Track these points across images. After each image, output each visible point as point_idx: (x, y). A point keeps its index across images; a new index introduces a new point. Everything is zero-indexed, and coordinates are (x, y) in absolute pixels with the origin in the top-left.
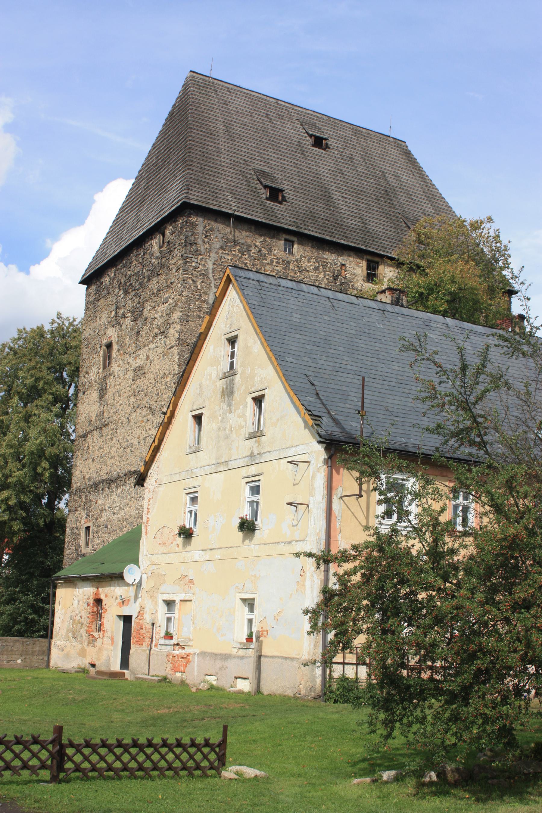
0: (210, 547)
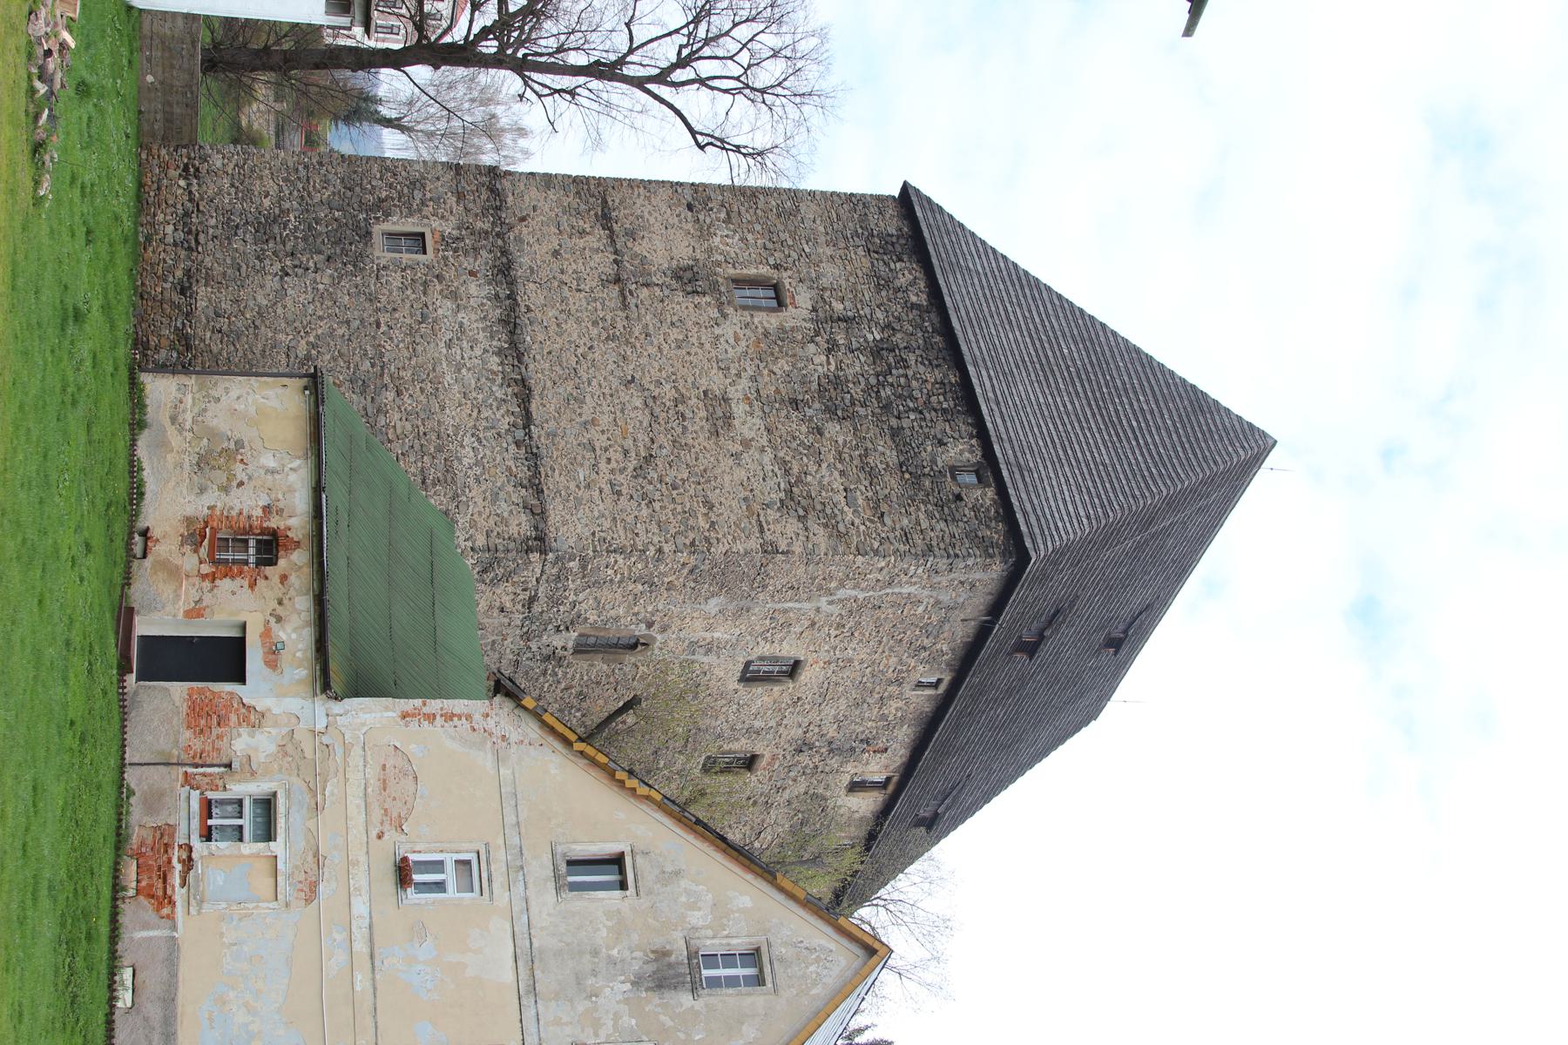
0: (377, 952)
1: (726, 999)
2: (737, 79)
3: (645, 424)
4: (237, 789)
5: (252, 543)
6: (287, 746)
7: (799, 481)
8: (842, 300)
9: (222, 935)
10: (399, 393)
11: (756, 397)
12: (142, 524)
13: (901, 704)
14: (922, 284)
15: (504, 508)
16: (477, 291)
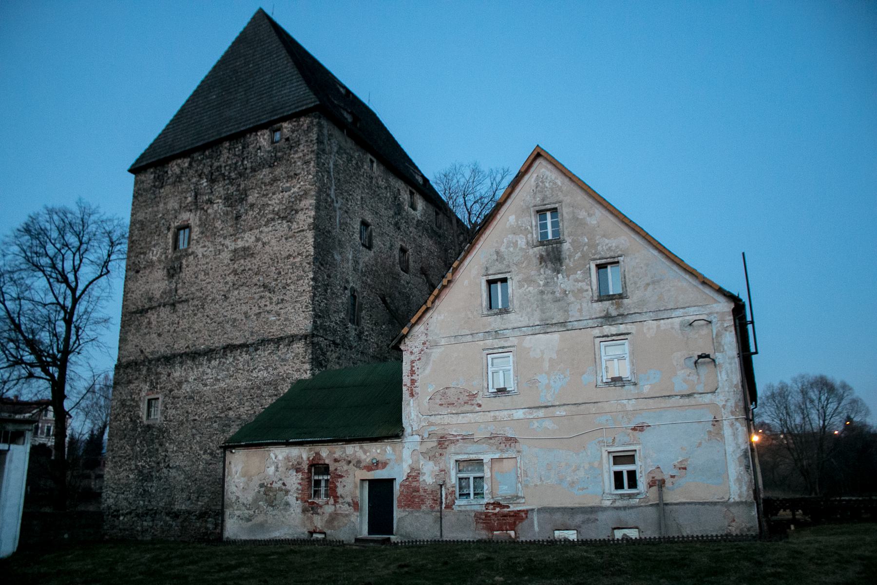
1: (566, 228)
2: (74, 254)
3: (247, 288)
4: (453, 479)
5: (316, 478)
6: (430, 456)
7: (277, 214)
8: (186, 198)
9: (536, 485)
10: (230, 409)
11: (234, 236)
12: (305, 536)
13: (380, 179)
14: (179, 161)
15: (290, 355)
16: (178, 373)
